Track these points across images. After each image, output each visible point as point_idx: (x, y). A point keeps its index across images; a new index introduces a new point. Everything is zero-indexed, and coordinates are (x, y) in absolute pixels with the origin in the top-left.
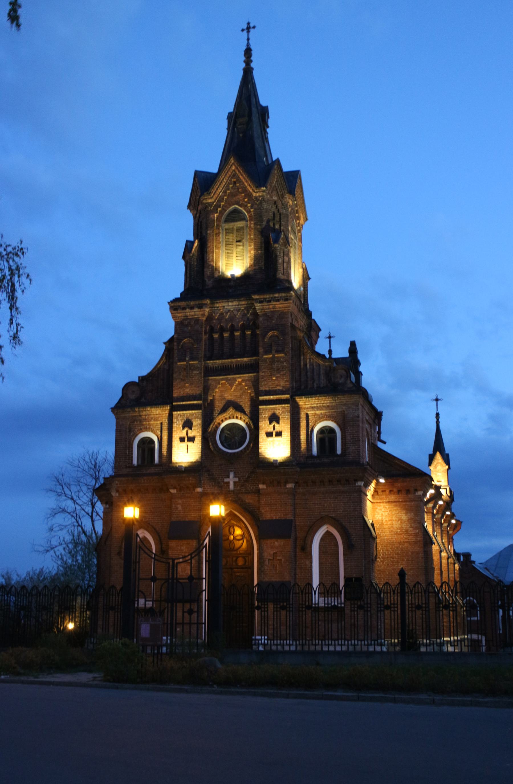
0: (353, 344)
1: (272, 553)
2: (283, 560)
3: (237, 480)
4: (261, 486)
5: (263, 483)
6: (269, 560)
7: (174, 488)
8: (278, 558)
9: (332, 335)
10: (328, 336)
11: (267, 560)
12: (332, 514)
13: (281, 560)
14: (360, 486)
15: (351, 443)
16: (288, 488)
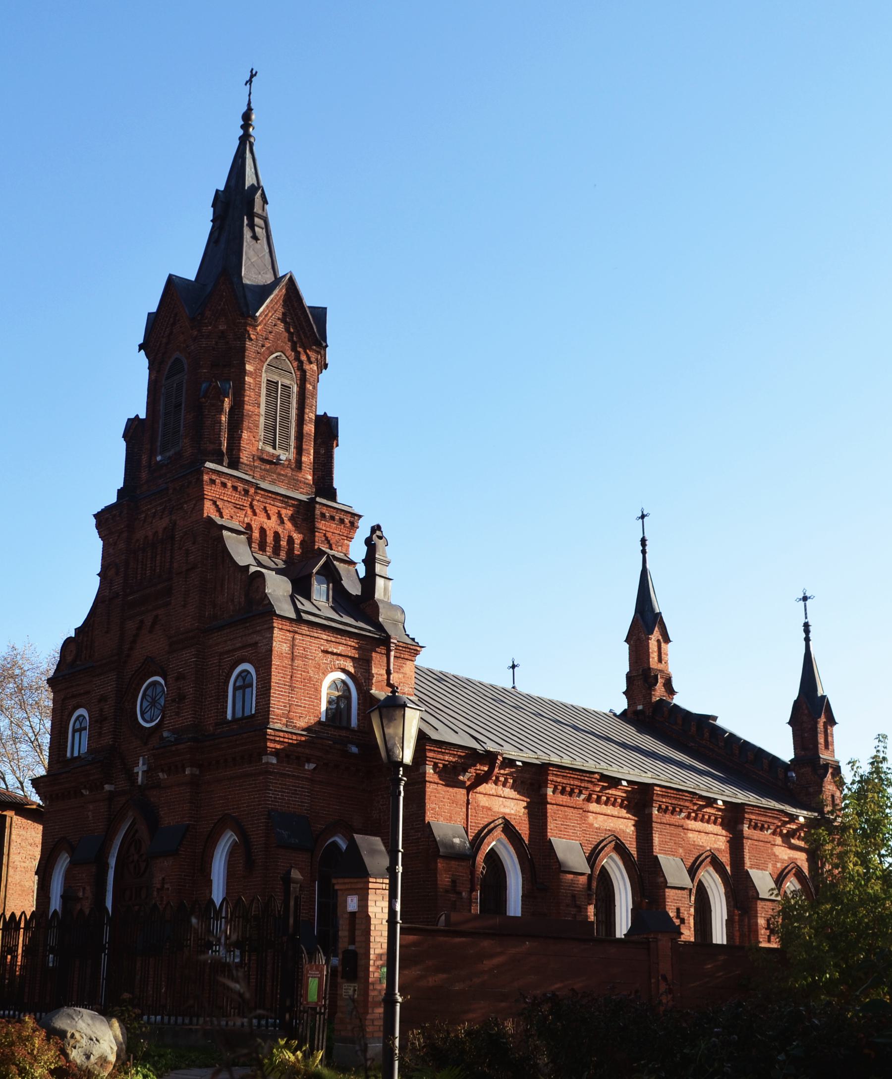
0: (376, 529)
1: (160, 878)
2: (170, 889)
3: (145, 768)
4: (161, 775)
5: (163, 771)
6: (158, 889)
7: (85, 788)
8: (166, 886)
9: (645, 513)
10: (640, 515)
11: (156, 889)
12: (235, 813)
13: (168, 889)
14: (267, 763)
15: (261, 695)
16: (186, 775)
